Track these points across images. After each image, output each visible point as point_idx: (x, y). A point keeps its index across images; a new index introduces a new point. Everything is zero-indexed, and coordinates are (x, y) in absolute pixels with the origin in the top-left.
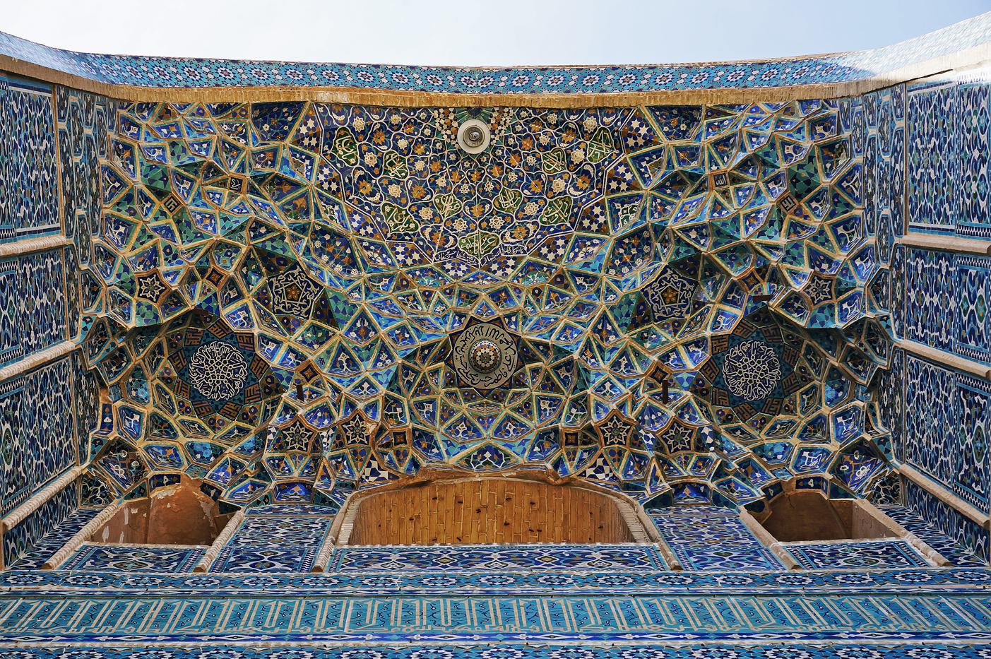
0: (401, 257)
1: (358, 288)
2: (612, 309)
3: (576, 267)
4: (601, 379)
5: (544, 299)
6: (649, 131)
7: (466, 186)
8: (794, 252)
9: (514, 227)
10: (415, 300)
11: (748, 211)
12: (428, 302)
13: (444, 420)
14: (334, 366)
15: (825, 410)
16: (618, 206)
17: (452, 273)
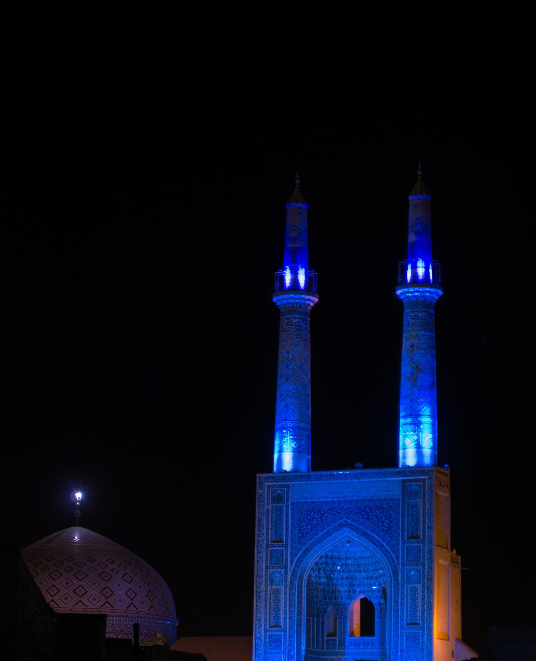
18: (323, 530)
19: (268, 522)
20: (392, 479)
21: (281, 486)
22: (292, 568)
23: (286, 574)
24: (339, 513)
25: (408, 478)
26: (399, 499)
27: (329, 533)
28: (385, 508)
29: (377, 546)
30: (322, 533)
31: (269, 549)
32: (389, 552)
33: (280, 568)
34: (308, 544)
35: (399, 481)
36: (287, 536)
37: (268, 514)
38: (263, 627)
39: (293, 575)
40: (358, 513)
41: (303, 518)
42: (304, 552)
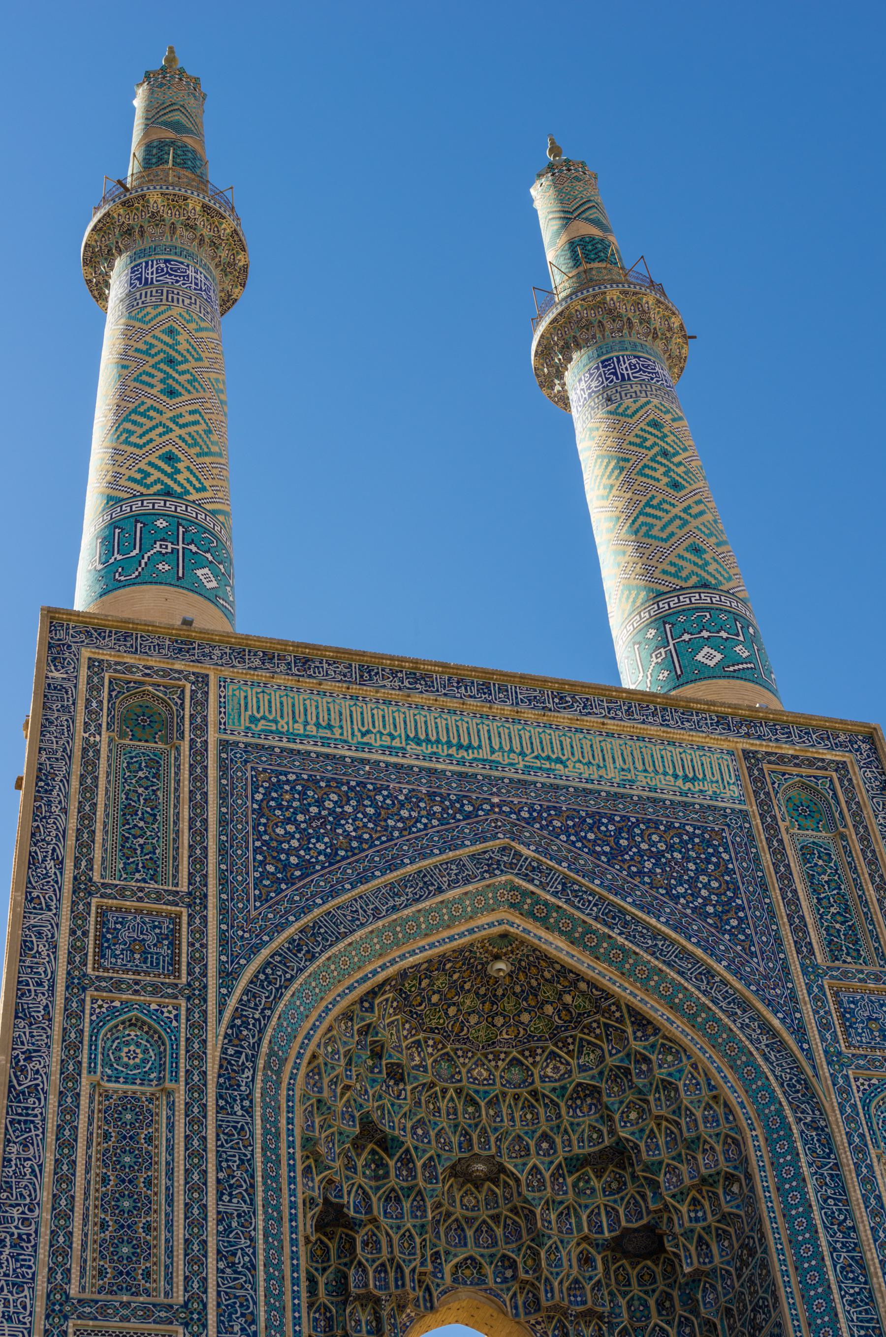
0: (430, 1050)
1: (405, 1114)
2: (566, 1159)
3: (547, 1093)
4: (551, 1242)
5: (520, 1105)
6: (622, 1016)
7: (484, 989)
8: (689, 1234)
9: (510, 1026)
10: (436, 1097)
11: (670, 1162)
12: (443, 1097)
13: (445, 1221)
14: (386, 1200)
15: (675, 1294)
16: (585, 1043)
17: (462, 1060)
18: (392, 868)
19: (88, 791)
20: (698, 738)
21: (166, 673)
22: (232, 1002)
23: (198, 1027)
24: (468, 816)
25: (772, 747)
26: (744, 814)
27: (426, 884)
28: (692, 836)
29: (681, 974)
30: (391, 876)
31: (94, 901)
32: (745, 1005)
33: (156, 990)
34: (317, 912)
35: (731, 753)
36: (198, 862)
37: (90, 764)
38: (42, 1285)
39: (234, 1036)
40: (566, 830)
41: (280, 807)
42: (295, 946)
